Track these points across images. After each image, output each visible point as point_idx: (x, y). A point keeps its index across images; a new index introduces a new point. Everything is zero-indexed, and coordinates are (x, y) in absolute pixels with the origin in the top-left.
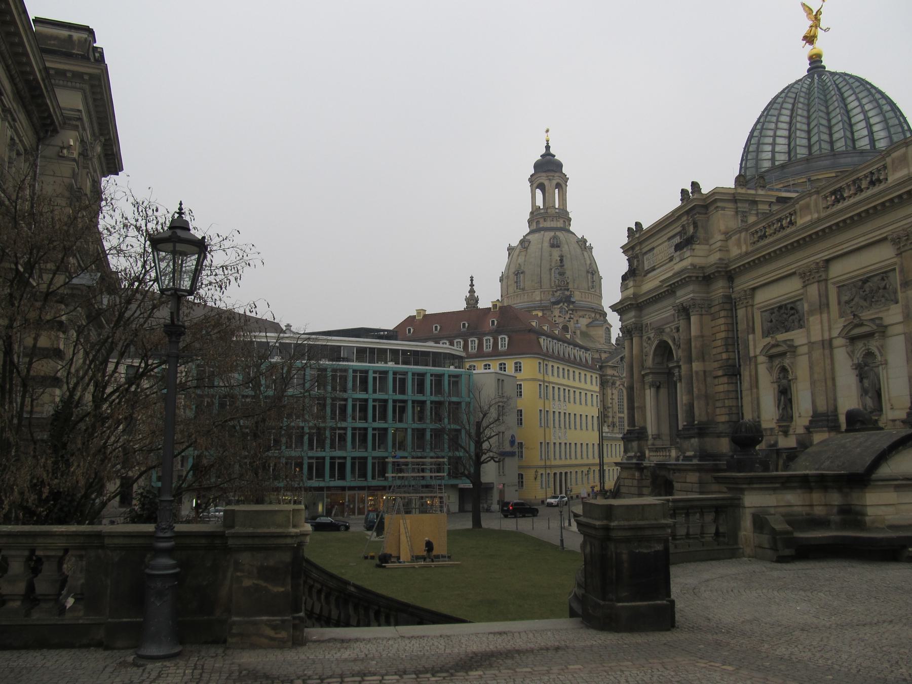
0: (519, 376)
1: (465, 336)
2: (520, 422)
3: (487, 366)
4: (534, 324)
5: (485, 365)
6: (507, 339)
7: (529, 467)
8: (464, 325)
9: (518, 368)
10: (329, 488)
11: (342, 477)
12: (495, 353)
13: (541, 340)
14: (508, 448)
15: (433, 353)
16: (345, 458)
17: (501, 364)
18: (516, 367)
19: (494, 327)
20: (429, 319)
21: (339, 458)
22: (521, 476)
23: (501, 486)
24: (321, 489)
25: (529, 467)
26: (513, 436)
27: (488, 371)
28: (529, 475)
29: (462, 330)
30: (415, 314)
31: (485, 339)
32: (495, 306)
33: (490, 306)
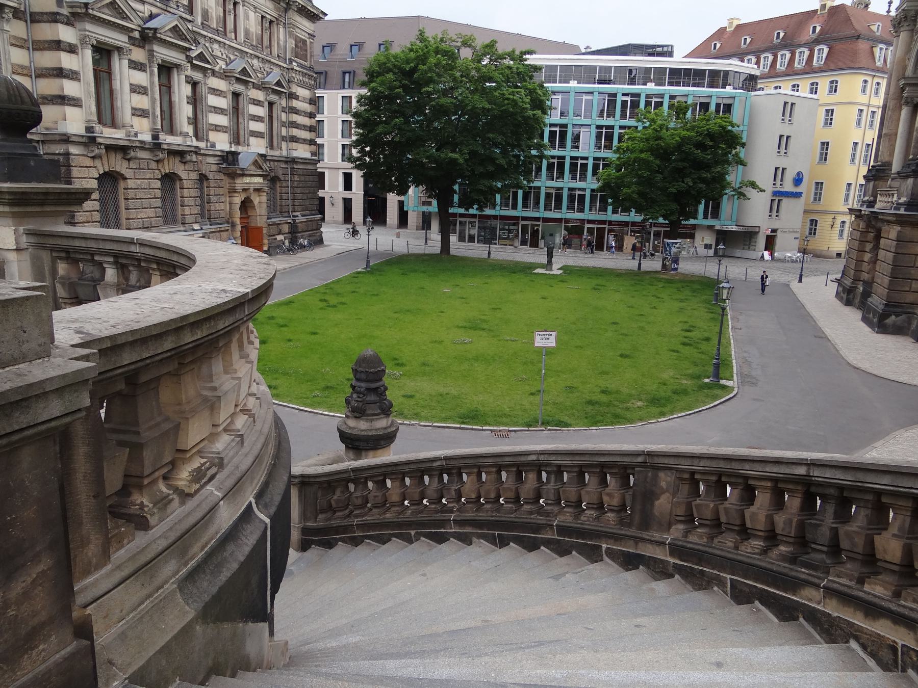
0: (834, 98)
1: (774, 49)
2: (824, 157)
3: (795, 87)
4: (874, 28)
5: (794, 86)
6: (826, 50)
7: (825, 212)
8: (778, 34)
9: (833, 88)
10: (567, 221)
11: (581, 210)
12: (809, 69)
13: (877, 51)
14: (788, 187)
15: (710, 71)
16: (584, 190)
17: (794, 86)
18: (831, 87)
19: (815, 36)
20: (741, 28)
21: (580, 189)
22: (814, 223)
23: (769, 232)
24: (559, 220)
25: (825, 212)
26: (798, 174)
27: (795, 93)
28: (824, 223)
29: (776, 41)
30: (725, 24)
31: (798, 51)
32: (823, 6)
33: (817, 6)
